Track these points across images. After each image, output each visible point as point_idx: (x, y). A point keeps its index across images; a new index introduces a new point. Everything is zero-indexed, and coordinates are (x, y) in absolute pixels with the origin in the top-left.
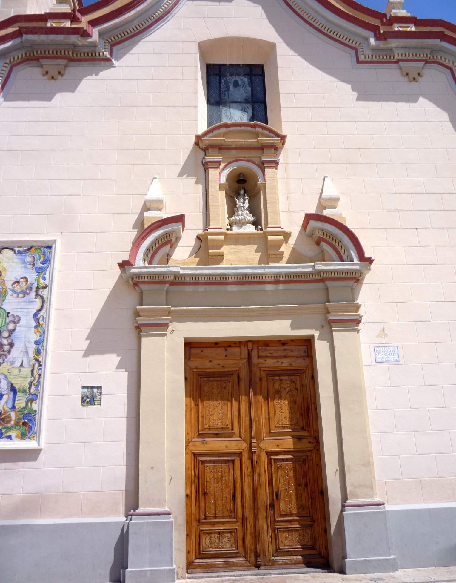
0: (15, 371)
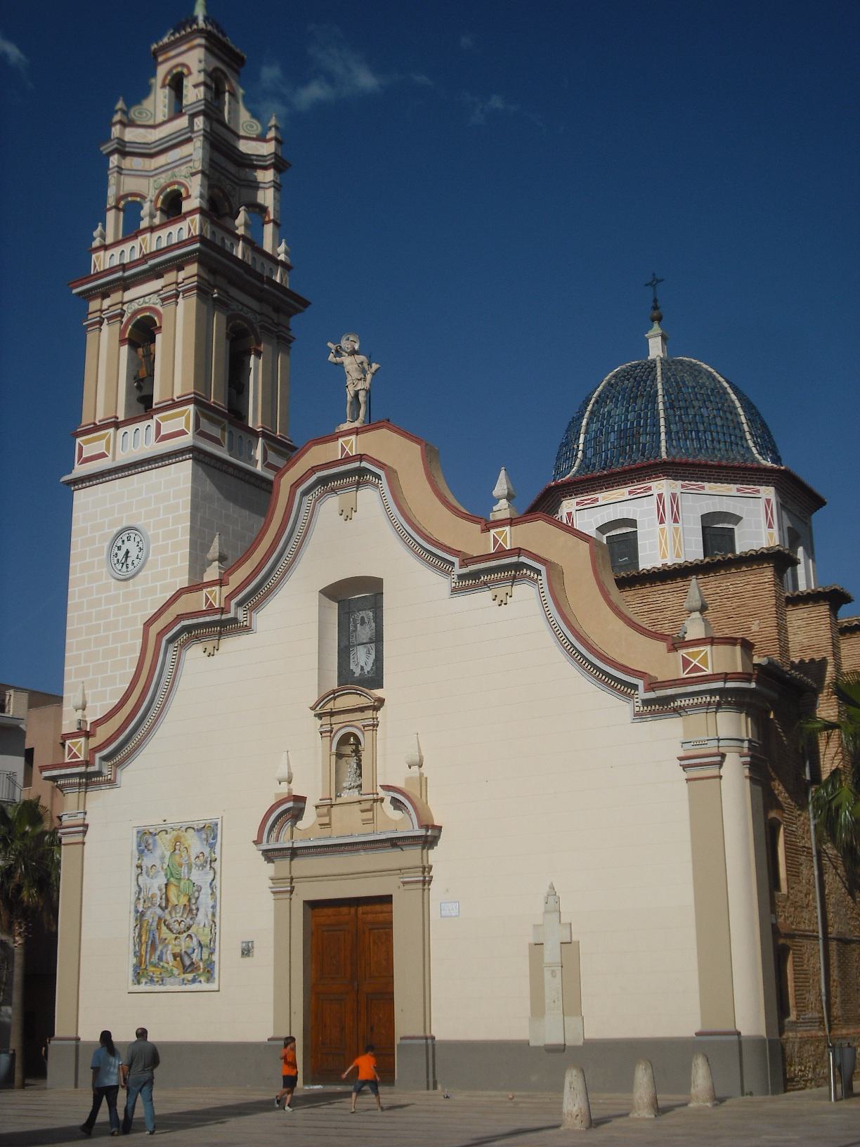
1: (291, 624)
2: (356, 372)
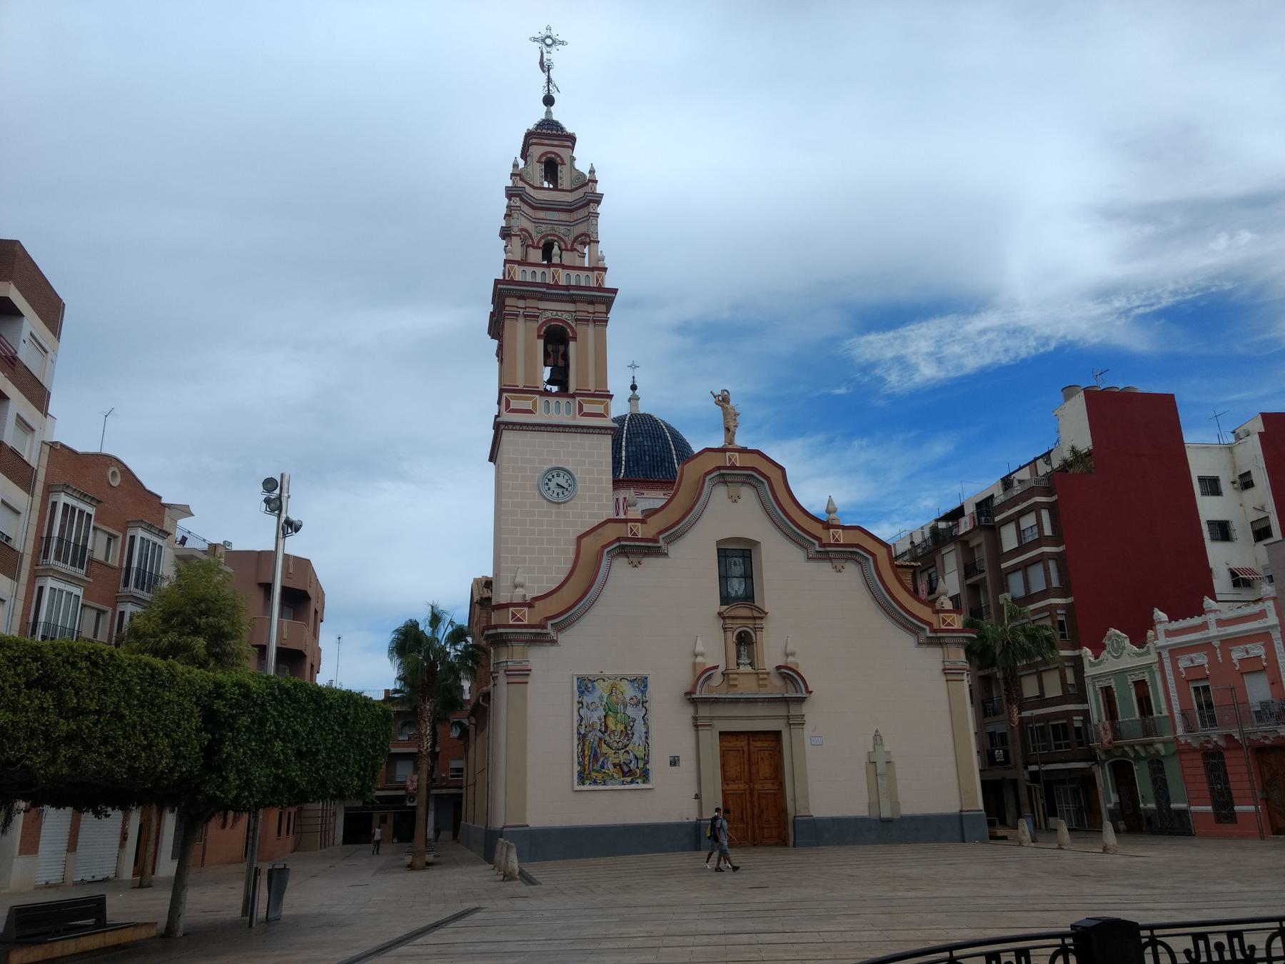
1: (694, 560)
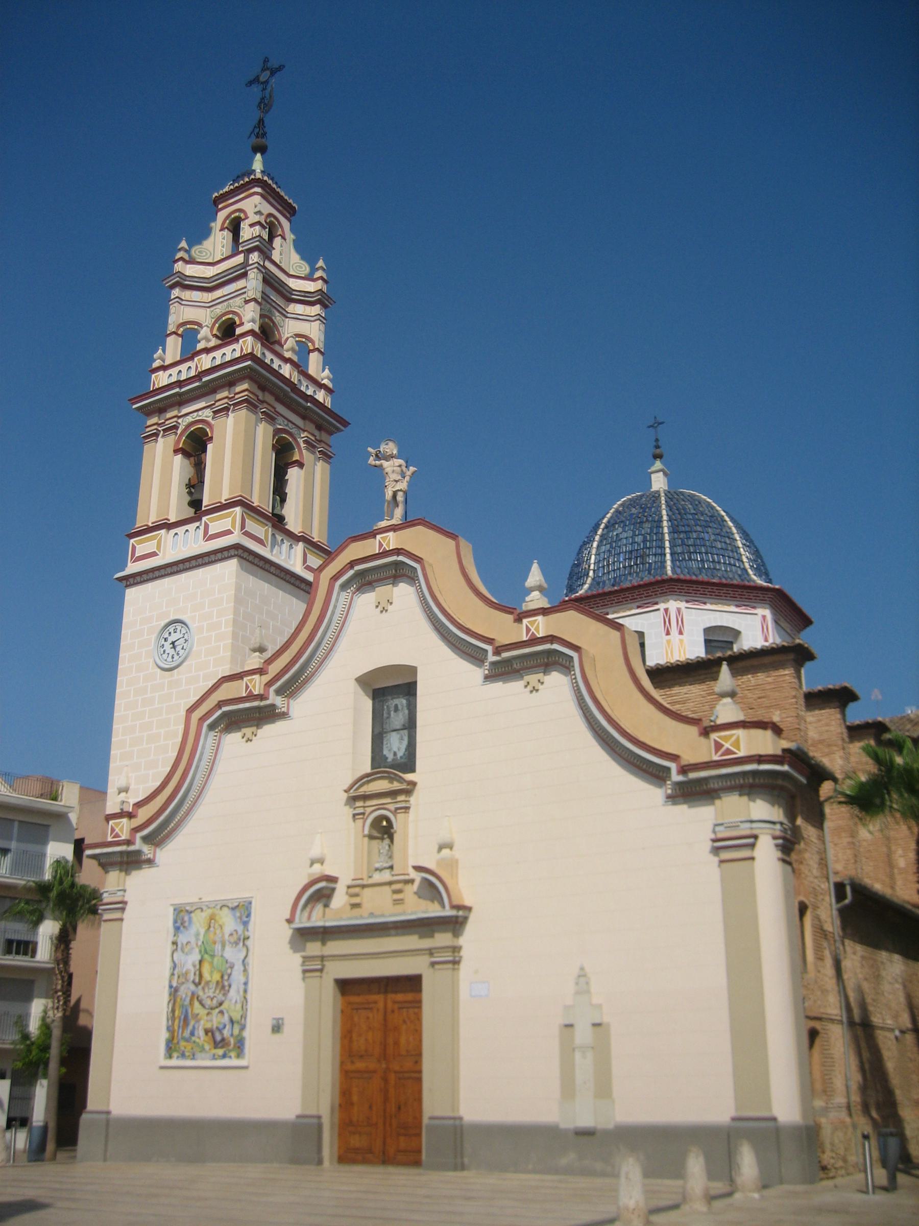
0: (232, 1007)
2: (396, 475)
